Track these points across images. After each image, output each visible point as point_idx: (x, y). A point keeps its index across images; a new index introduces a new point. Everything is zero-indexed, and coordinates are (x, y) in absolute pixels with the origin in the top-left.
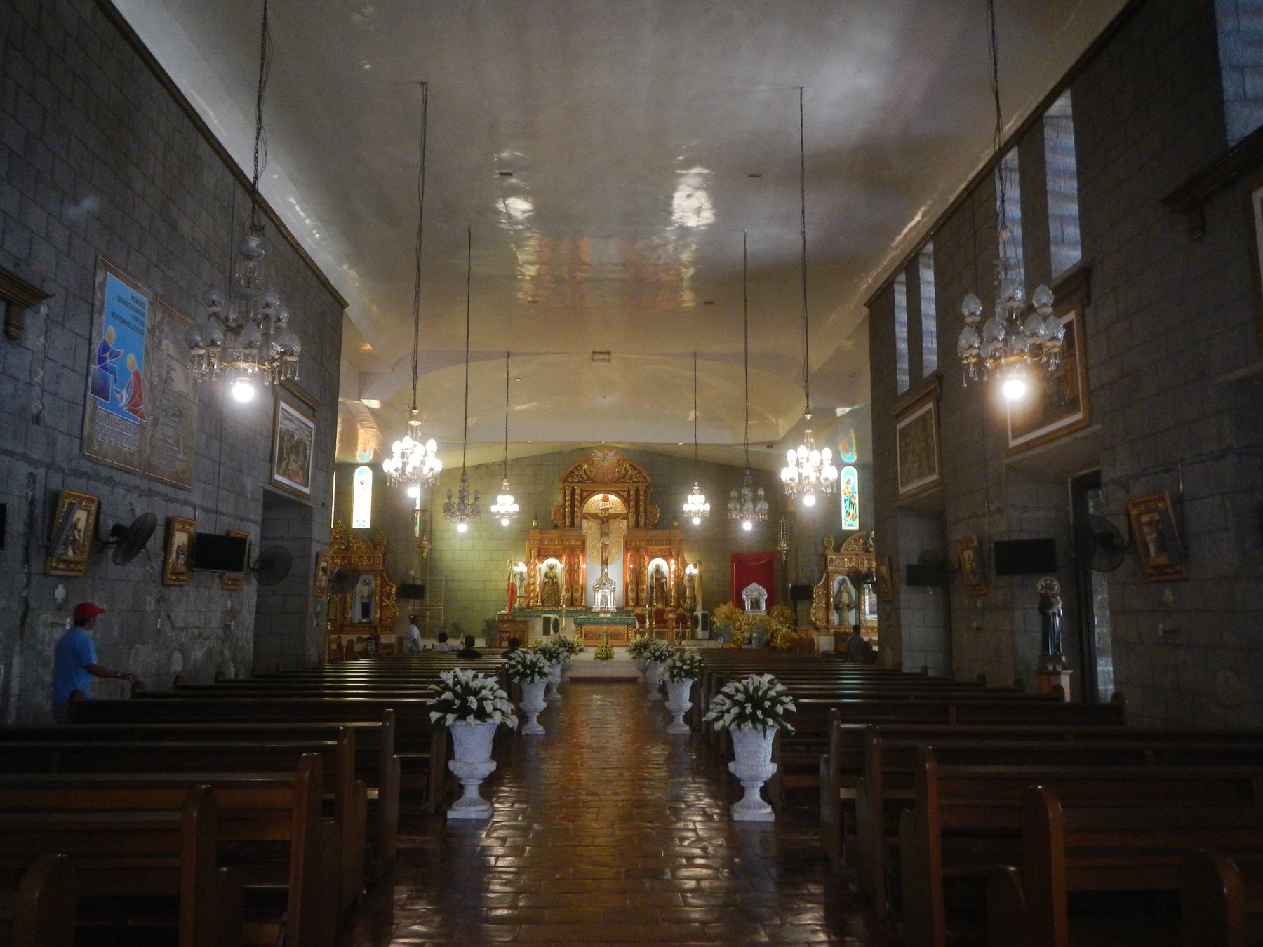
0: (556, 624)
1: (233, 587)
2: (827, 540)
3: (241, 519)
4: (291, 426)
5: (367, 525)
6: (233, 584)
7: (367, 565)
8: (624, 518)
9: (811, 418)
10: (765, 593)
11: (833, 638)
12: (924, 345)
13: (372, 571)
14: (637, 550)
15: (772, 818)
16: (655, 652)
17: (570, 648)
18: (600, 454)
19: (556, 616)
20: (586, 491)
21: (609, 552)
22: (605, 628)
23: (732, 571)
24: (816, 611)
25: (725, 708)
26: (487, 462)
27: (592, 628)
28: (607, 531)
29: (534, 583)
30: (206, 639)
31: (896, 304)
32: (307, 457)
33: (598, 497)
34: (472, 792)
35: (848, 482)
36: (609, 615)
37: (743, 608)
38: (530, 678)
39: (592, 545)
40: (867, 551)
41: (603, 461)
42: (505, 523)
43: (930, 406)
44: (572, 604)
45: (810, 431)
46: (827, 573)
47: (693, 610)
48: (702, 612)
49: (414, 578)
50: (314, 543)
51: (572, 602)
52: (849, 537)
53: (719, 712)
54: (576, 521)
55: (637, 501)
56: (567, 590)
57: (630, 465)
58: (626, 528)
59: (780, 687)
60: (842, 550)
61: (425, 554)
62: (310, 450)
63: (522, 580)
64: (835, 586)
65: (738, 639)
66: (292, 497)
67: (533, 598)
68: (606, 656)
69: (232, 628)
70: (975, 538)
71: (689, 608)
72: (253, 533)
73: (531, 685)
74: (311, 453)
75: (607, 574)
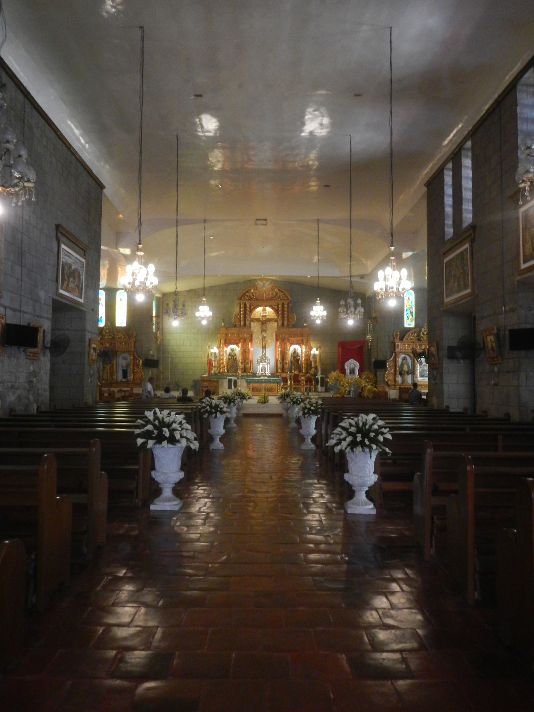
0: (236, 382)
1: (34, 358)
2: (396, 334)
3: (38, 316)
4: (70, 261)
5: (126, 326)
6: (34, 356)
7: (125, 348)
8: (275, 321)
9: (394, 249)
10: (358, 365)
11: (398, 391)
12: (464, 207)
13: (128, 352)
14: (283, 340)
15: (374, 512)
16: (293, 399)
17: (243, 396)
18: (261, 283)
19: (236, 378)
20: (252, 305)
21: (266, 342)
22: (264, 385)
23: (339, 352)
24: (388, 375)
25: (342, 437)
27: (256, 385)
28: (265, 328)
29: (223, 359)
30: (16, 389)
31: (445, 183)
32: (81, 280)
33: (260, 309)
34: (167, 492)
35: (409, 299)
36: (266, 378)
37: (345, 373)
38: (215, 415)
39: (256, 337)
40: (419, 340)
41: (263, 287)
42: (204, 322)
43: (467, 246)
44: (245, 371)
45: (393, 258)
46: (395, 353)
47: (316, 374)
48: (321, 376)
49: (152, 356)
50: (87, 333)
51: (245, 370)
52: (408, 332)
53: (337, 440)
54: (247, 323)
55: (283, 310)
56: (242, 363)
57: (279, 290)
58: (276, 327)
59: (381, 423)
60: (404, 339)
61: (158, 342)
62: (83, 276)
63: (216, 357)
64: (400, 360)
65: (342, 392)
66: (72, 304)
67: (222, 368)
68: (264, 401)
69: (34, 382)
70: (495, 328)
71: (313, 373)
72: (46, 325)
73: (216, 419)
74: (83, 278)
75: (265, 354)
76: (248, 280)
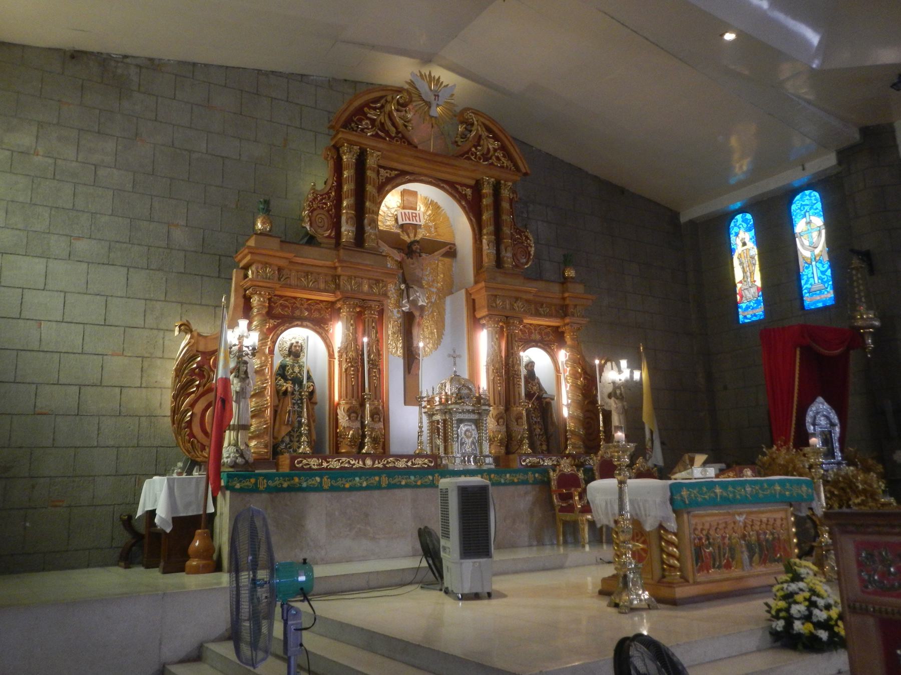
57: (489, 130)
76: (346, 80)
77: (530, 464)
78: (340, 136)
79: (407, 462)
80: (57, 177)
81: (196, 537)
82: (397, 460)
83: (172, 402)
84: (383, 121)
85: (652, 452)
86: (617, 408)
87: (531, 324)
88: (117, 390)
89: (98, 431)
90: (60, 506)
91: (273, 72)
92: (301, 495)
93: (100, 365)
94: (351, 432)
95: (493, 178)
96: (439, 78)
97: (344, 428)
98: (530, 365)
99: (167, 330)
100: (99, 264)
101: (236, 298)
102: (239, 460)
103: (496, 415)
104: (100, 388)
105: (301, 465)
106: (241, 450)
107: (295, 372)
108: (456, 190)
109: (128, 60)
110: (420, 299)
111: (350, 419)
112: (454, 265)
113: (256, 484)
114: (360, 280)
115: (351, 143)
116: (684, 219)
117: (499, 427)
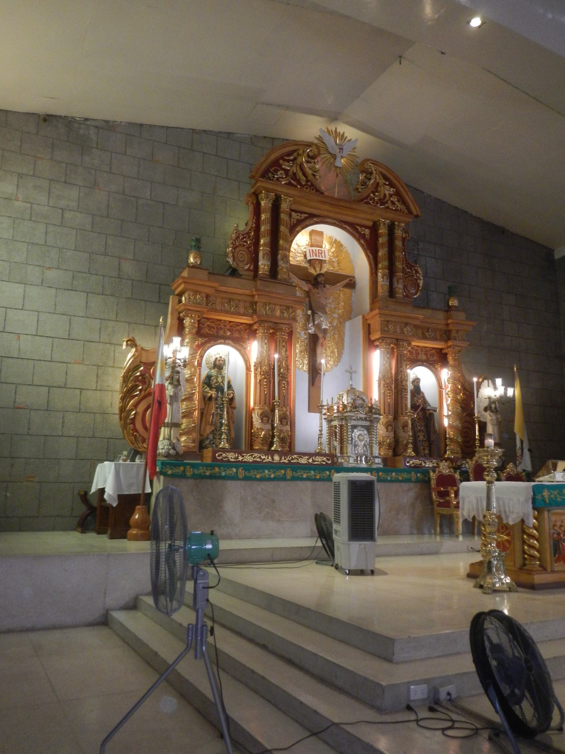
26: (68, 115)
57: (385, 178)
76: (265, 137)
77: (413, 465)
78: (259, 184)
79: (308, 459)
80: (33, 219)
81: (136, 511)
82: (300, 457)
83: (120, 403)
84: (295, 171)
85: (521, 459)
86: (491, 420)
87: (418, 346)
88: (78, 392)
89: (63, 423)
90: (32, 481)
91: (205, 131)
92: (220, 482)
93: (65, 371)
94: (263, 433)
95: (388, 220)
96: (344, 133)
97: (258, 429)
98: (416, 381)
99: (117, 344)
100: (65, 289)
101: (172, 319)
102: (172, 452)
103: (386, 423)
104: (64, 390)
105: (221, 457)
106: (173, 444)
107: (218, 382)
108: (357, 230)
109: (88, 123)
110: (323, 323)
111: (262, 421)
112: (353, 294)
113: (184, 471)
114: (274, 306)
115: (268, 191)
116: (557, 256)
117: (387, 433)
